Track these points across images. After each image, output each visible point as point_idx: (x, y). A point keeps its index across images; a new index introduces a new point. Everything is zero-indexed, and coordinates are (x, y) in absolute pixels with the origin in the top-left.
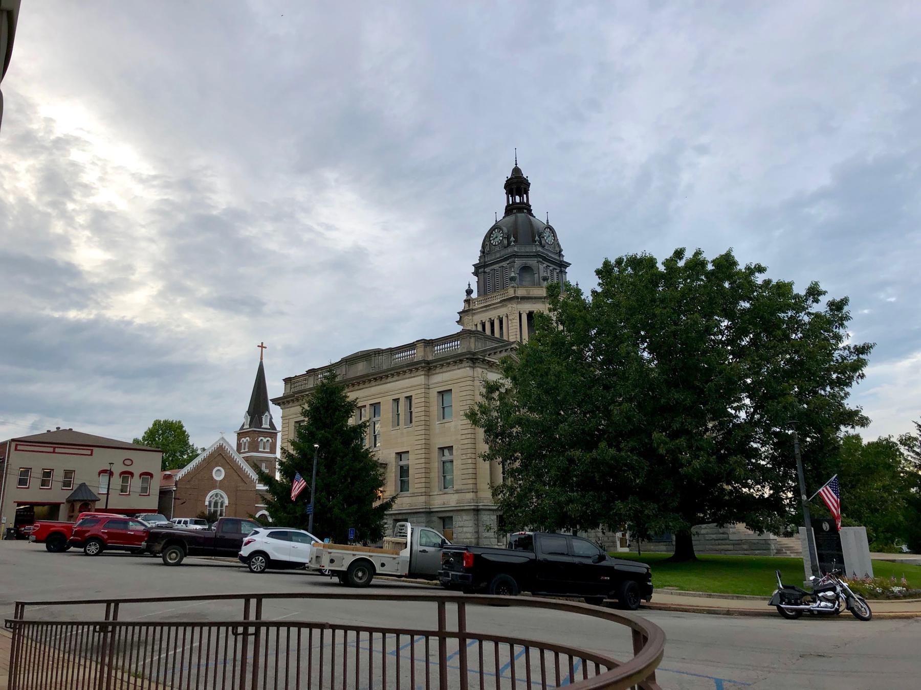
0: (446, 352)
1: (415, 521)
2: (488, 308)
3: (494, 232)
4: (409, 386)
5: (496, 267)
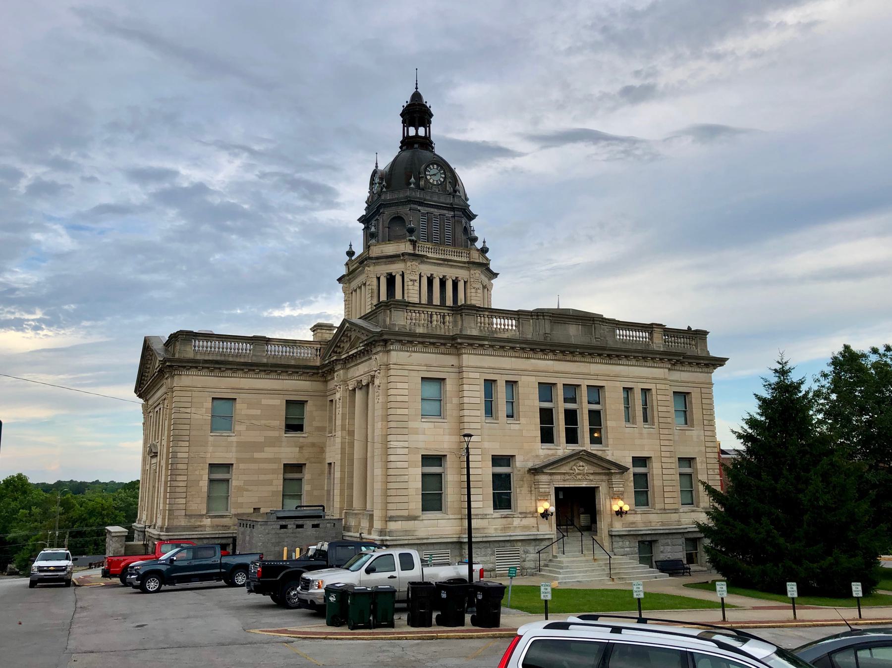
0: (670, 347)
1: (670, 543)
2: (446, 263)
4: (651, 376)
5: (436, 212)
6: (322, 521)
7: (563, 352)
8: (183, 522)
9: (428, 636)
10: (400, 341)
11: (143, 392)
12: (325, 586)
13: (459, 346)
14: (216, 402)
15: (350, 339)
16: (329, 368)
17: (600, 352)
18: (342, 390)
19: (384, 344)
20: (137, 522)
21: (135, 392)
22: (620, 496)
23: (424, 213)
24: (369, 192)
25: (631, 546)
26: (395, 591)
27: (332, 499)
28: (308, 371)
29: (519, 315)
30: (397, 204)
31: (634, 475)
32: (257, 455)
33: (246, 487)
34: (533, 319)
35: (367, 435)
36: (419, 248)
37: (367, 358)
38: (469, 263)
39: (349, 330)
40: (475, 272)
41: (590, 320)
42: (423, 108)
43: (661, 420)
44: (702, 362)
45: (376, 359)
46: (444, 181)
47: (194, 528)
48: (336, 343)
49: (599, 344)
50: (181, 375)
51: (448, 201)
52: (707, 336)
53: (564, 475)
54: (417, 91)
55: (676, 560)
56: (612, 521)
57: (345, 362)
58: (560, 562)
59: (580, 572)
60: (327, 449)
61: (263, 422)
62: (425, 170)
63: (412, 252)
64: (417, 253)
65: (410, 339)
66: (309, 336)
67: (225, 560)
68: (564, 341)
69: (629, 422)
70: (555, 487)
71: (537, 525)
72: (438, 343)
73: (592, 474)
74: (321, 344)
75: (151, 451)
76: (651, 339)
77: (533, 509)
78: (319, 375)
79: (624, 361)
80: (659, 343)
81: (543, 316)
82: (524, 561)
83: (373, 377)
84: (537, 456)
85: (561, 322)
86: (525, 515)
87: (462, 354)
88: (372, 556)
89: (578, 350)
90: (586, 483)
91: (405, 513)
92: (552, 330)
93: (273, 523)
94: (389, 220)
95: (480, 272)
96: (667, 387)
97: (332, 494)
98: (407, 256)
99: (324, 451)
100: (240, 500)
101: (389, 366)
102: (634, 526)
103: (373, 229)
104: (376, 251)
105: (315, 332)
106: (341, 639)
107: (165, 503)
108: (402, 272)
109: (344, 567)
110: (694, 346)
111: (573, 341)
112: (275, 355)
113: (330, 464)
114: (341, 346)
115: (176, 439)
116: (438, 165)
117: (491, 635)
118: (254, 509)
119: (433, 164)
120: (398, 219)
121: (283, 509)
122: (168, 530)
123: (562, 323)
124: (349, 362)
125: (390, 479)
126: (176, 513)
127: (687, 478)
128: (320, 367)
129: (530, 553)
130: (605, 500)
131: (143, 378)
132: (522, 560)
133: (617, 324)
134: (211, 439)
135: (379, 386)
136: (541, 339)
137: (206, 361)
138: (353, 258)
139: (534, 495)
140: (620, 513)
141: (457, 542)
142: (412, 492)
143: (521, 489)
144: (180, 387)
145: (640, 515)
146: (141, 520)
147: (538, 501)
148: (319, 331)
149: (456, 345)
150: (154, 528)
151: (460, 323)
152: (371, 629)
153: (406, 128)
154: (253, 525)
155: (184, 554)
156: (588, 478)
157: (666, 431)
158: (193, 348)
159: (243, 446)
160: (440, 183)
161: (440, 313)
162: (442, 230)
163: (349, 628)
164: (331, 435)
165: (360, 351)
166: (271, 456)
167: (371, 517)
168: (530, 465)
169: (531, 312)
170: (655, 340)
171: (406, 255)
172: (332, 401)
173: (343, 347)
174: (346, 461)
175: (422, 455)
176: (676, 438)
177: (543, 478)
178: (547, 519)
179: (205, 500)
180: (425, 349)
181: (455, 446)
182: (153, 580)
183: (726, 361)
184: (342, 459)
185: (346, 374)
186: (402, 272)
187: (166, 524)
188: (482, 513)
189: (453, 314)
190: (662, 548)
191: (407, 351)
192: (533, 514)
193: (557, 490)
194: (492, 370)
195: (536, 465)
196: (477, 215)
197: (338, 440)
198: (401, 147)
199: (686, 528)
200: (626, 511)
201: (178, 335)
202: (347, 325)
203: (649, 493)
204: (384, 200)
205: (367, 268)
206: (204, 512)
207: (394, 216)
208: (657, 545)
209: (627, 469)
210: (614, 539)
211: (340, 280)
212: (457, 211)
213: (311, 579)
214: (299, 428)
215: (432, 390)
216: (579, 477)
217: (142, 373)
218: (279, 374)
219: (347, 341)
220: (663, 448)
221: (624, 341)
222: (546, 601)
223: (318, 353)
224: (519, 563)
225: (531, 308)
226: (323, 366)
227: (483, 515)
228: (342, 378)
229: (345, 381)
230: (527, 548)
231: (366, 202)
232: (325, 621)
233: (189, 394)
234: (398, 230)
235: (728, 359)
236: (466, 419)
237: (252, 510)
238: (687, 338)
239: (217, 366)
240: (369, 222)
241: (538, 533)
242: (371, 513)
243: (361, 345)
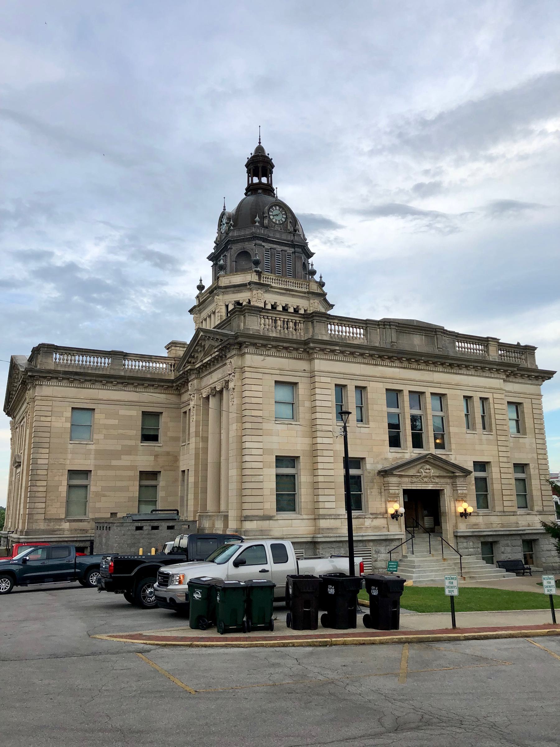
2: (288, 292)
4: (488, 386)
5: (279, 248)
6: (177, 523)
7: (409, 360)
8: (42, 526)
9: (320, 642)
10: (254, 345)
11: (10, 409)
12: (188, 580)
13: (311, 351)
14: (76, 412)
15: (204, 348)
16: (183, 380)
17: (443, 361)
18: (195, 399)
19: (239, 347)
20: (3, 529)
21: (4, 411)
22: (462, 498)
23: (267, 248)
24: (217, 232)
25: (474, 547)
26: (274, 586)
27: (185, 505)
28: (163, 384)
29: (366, 324)
30: (243, 240)
31: (476, 479)
32: (114, 463)
33: (103, 492)
34: (379, 328)
35: (221, 440)
36: (263, 279)
37: (221, 364)
38: (308, 293)
39: (203, 339)
40: (314, 301)
41: (432, 331)
42: (266, 159)
43: (499, 427)
44: (533, 374)
45: (231, 362)
46: (285, 221)
47: (53, 532)
48: (190, 353)
49: (441, 353)
50: (41, 385)
51: (289, 238)
52: (535, 351)
53: (412, 477)
54: (260, 145)
55: (516, 561)
56: (456, 523)
57: (199, 372)
58: (413, 562)
59: (432, 571)
60: (181, 458)
61: (120, 431)
62: (269, 211)
63: (258, 281)
64: (263, 282)
65: (265, 342)
66: (165, 353)
67: (80, 560)
68: (407, 348)
69: (469, 429)
70: (403, 489)
71: (387, 526)
72: (291, 347)
73: (438, 477)
74: (175, 360)
75: (16, 462)
76: (487, 352)
77: (383, 510)
78: (173, 388)
79: (464, 371)
80: (494, 354)
81: (390, 325)
82: (376, 561)
83: (227, 382)
84: (386, 459)
85: (406, 332)
86: (375, 516)
87: (314, 359)
88: (240, 546)
89: (423, 358)
90: (432, 486)
91: (260, 513)
92: (398, 338)
93: (129, 524)
94: (236, 255)
95: (318, 302)
96: (502, 396)
97: (185, 499)
98: (253, 285)
99: (178, 459)
100: (98, 505)
101: (244, 369)
102: (476, 527)
103: (222, 262)
104: (224, 281)
105: (170, 349)
106: (212, 646)
107: (25, 507)
108: (249, 299)
109: (207, 560)
110: (524, 360)
111: (417, 349)
112: (132, 368)
113: (184, 471)
114: (195, 356)
115: (36, 446)
116: (280, 207)
117: (397, 640)
118: (111, 514)
119: (275, 205)
120: (245, 254)
121: (139, 512)
122: (27, 533)
123: (406, 333)
124: (202, 371)
125: (246, 479)
126: (36, 517)
127: (522, 483)
128: (174, 380)
129: (381, 553)
130: (450, 502)
131: (11, 396)
132: (374, 560)
133: (456, 336)
134: (70, 446)
135: (234, 389)
136: (389, 346)
137: (66, 373)
138: (203, 292)
139: (383, 497)
140: (464, 515)
141: (311, 542)
142: (266, 492)
143: (372, 490)
144: (41, 396)
145: (481, 517)
146: (7, 528)
147: (388, 502)
148: (173, 348)
149: (308, 350)
150: (16, 533)
151: (311, 330)
152: (245, 632)
153: (250, 178)
154: (110, 527)
155: (40, 554)
156: (434, 481)
157: (503, 438)
158: (54, 360)
159: (100, 453)
161: (292, 320)
162: (284, 265)
163: (218, 632)
164: (184, 444)
165: (214, 358)
166: (128, 463)
167: (226, 518)
168: (380, 467)
169: (379, 322)
170: (491, 353)
171: (253, 284)
172: (185, 413)
173: (197, 357)
174: (200, 466)
175: (276, 456)
176: (511, 445)
177: (393, 480)
178: (397, 520)
179: (64, 504)
180: (278, 354)
181: (307, 448)
182: (4, 581)
183: (554, 374)
184: (196, 464)
185: (200, 382)
186: (249, 299)
187: (26, 528)
188: (335, 514)
189: (304, 321)
190: (502, 549)
191: (261, 355)
192: (383, 515)
193: (405, 492)
194: (342, 375)
195: (385, 468)
196: (314, 253)
197: (192, 446)
198: (246, 194)
199: (525, 530)
200: (470, 513)
201: (40, 347)
202: (202, 333)
203: (489, 496)
204: (232, 237)
205: (216, 297)
206: (63, 516)
207: (241, 251)
208: (498, 545)
209: (469, 473)
210: (460, 540)
211: (191, 311)
212: (297, 248)
213: (171, 573)
214: (154, 438)
215: (284, 394)
216: (425, 480)
217: (10, 392)
218: (136, 387)
219: (201, 351)
220: (501, 454)
221: (463, 352)
222: (452, 597)
223: (173, 368)
224: (370, 563)
225: (378, 318)
226: (177, 379)
227: (336, 515)
228: (196, 387)
229: (199, 390)
230: (378, 548)
231: (215, 242)
232: (187, 623)
233: (50, 403)
234: (243, 263)
235: (555, 372)
236: (318, 422)
237: (109, 515)
238: (517, 353)
239: (77, 377)
240: (218, 259)
241: (389, 533)
242: (226, 514)
243: (216, 350)
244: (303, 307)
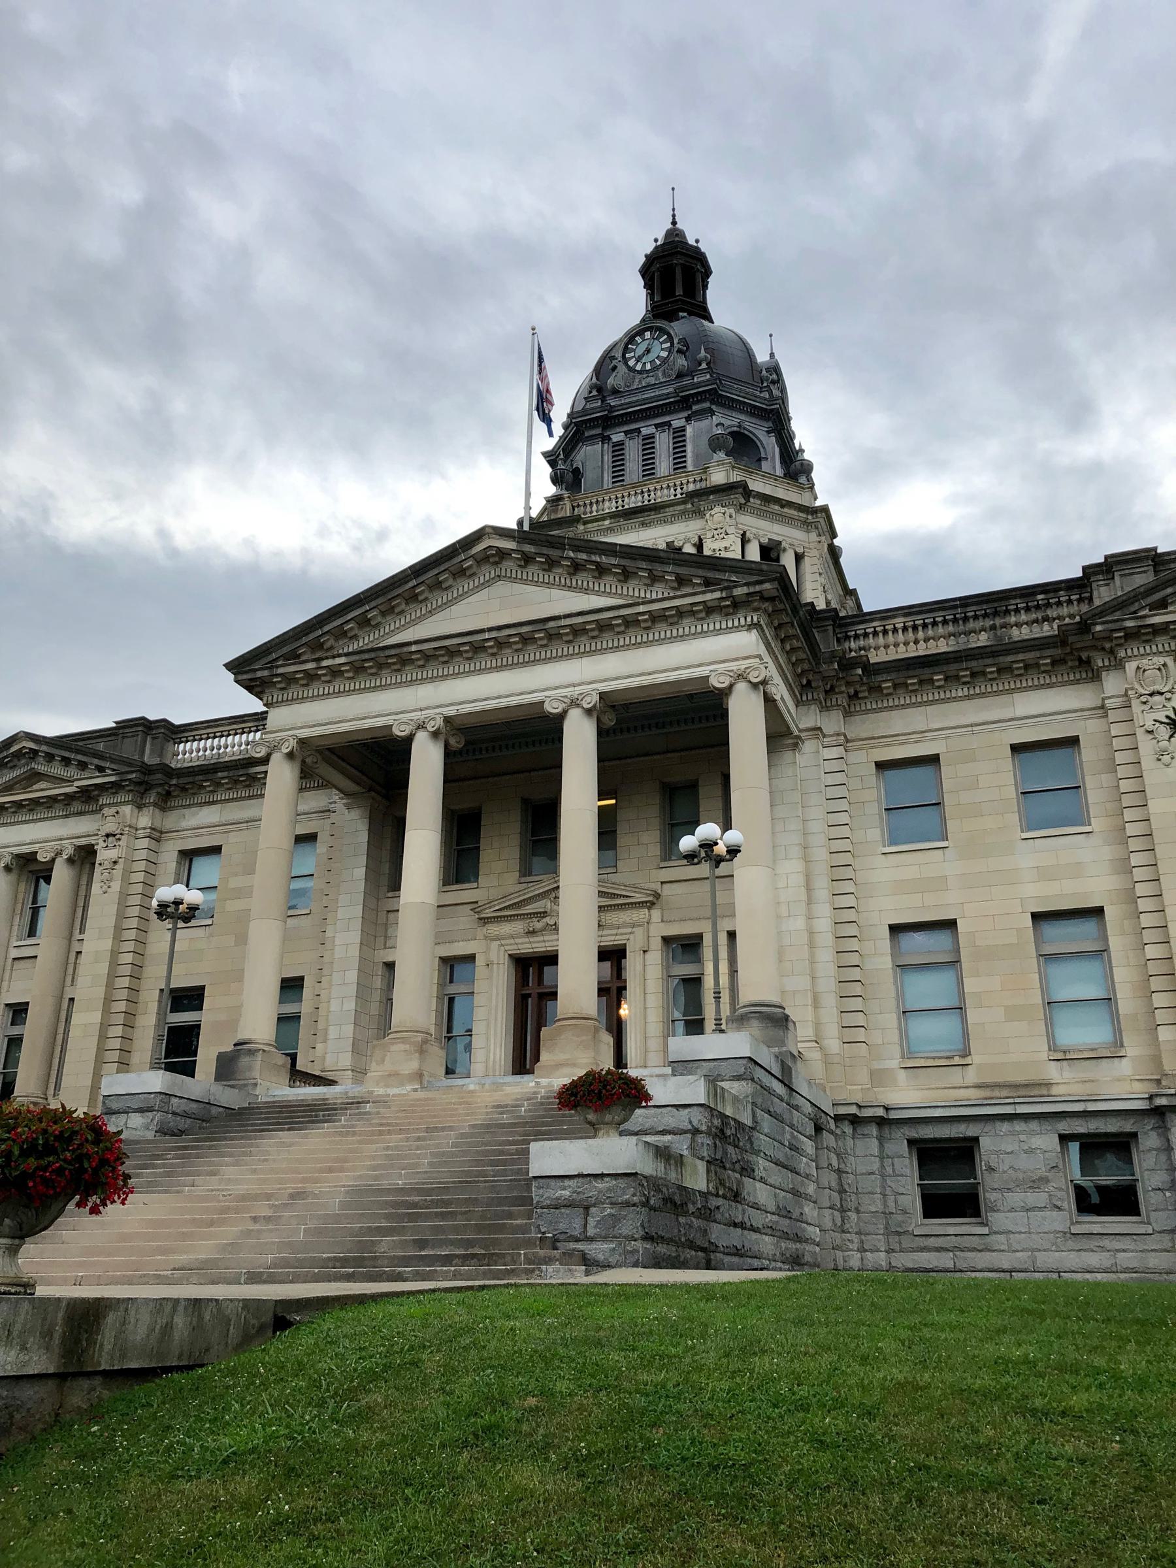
3: (638, 339)
160: (658, 362)
244: (687, 540)
